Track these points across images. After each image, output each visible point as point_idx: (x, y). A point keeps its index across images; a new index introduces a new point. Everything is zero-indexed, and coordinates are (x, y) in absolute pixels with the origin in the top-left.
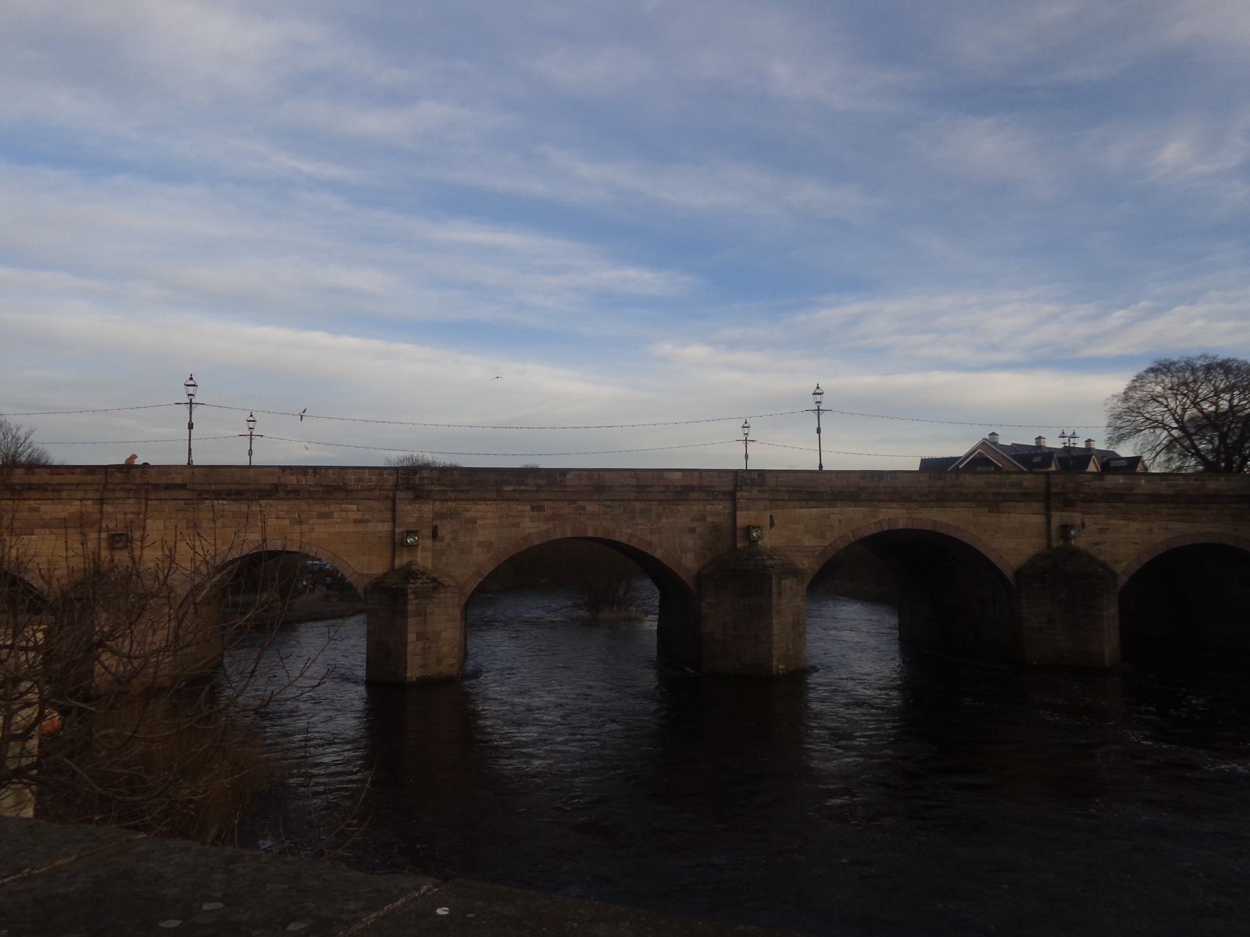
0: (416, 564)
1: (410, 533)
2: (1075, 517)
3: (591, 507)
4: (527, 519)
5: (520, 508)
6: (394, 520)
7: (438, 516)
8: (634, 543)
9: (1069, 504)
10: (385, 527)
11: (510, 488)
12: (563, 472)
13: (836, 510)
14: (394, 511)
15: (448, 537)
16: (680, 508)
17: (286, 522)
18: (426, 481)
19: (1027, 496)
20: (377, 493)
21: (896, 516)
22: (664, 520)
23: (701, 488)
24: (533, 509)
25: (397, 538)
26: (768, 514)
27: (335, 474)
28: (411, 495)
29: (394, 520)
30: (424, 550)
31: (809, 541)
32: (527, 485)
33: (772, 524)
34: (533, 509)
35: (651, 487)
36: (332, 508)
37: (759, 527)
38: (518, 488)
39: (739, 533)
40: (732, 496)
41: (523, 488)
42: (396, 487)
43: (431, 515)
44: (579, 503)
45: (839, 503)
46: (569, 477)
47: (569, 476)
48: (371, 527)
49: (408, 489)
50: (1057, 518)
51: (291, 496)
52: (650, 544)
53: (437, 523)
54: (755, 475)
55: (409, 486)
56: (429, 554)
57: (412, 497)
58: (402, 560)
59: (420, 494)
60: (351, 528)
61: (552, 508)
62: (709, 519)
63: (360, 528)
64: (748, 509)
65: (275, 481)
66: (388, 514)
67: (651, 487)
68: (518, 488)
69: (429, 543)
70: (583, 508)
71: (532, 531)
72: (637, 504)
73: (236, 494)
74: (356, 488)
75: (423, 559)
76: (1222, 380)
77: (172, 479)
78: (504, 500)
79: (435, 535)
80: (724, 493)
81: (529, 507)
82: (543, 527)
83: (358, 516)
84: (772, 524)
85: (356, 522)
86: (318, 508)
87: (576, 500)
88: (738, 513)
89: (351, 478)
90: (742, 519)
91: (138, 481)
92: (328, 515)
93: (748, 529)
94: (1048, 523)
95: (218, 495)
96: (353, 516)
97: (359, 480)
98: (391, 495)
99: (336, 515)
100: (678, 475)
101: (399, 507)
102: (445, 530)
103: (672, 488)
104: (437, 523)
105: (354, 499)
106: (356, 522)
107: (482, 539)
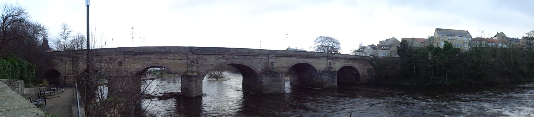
0: (193, 69)
1: (192, 62)
2: (331, 61)
3: (236, 57)
4: (221, 59)
5: (220, 57)
7: (198, 58)
8: (248, 65)
9: (330, 59)
10: (186, 61)
11: (217, 52)
12: (230, 49)
13: (290, 59)
15: (200, 63)
16: (257, 58)
18: (195, 50)
19: (324, 57)
21: (301, 60)
22: (254, 60)
23: (261, 54)
24: (223, 57)
25: (189, 63)
26: (275, 59)
28: (192, 53)
30: (195, 66)
32: (221, 51)
33: (276, 62)
34: (223, 57)
35: (251, 53)
37: (273, 62)
38: (219, 52)
41: (220, 52)
43: (196, 58)
44: (233, 56)
45: (291, 57)
46: (231, 50)
47: (231, 50)
48: (182, 61)
49: (191, 52)
50: (329, 61)
52: (251, 66)
53: (198, 60)
54: (273, 51)
55: (191, 51)
56: (196, 67)
57: (192, 53)
58: (190, 69)
59: (194, 54)
61: (227, 57)
62: (263, 60)
64: (271, 58)
66: (187, 58)
67: (251, 53)
68: (219, 52)
69: (196, 64)
70: (234, 57)
71: (222, 62)
72: (248, 57)
75: (194, 69)
76: (320, 39)
78: (216, 55)
79: (197, 63)
80: (266, 55)
81: (221, 57)
82: (225, 61)
83: (179, 58)
84: (276, 62)
85: (179, 59)
87: (232, 55)
88: (270, 59)
90: (270, 60)
93: (272, 63)
94: (327, 62)
95: (140, 54)
96: (178, 58)
100: (257, 50)
101: (189, 56)
102: (199, 62)
103: (256, 53)
104: (198, 60)
105: (178, 54)
106: (179, 59)
107: (211, 64)
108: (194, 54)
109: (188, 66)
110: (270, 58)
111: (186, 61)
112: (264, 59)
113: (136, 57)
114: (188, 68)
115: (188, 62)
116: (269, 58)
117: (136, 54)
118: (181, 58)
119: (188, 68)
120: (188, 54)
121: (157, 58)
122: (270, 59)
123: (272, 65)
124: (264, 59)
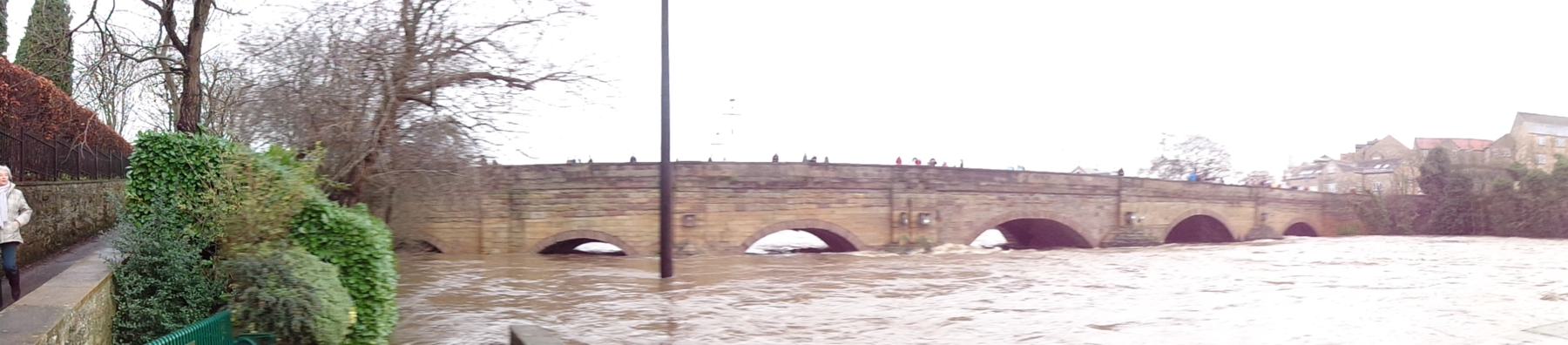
6: (891, 204)
10: (884, 211)
14: (890, 198)
17: (814, 206)
20: (877, 185)
27: (848, 170)
28: (902, 185)
29: (891, 204)
31: (1162, 222)
36: (848, 195)
39: (1122, 217)
40: (1117, 193)
42: (892, 180)
48: (874, 210)
49: (900, 181)
51: (819, 186)
60: (860, 211)
63: (867, 211)
65: (805, 175)
66: (886, 201)
73: (771, 186)
74: (866, 180)
77: (724, 173)
83: (865, 202)
86: (837, 195)
89: (860, 172)
90: (1125, 207)
91: (700, 174)
92: (843, 202)
93: (1129, 213)
97: (866, 175)
98: (888, 185)
99: (850, 201)
101: (896, 195)
108: (909, 188)
109: (892, 228)
110: (1125, 201)
111: (884, 211)
112: (1108, 204)
113: (744, 197)
114: (891, 234)
115: (891, 215)
116: (1120, 201)
117: (746, 186)
118: (872, 202)
119: (891, 234)
120: (890, 189)
121: (812, 200)
122: (1123, 204)
123: (1129, 222)
124: (1108, 204)
